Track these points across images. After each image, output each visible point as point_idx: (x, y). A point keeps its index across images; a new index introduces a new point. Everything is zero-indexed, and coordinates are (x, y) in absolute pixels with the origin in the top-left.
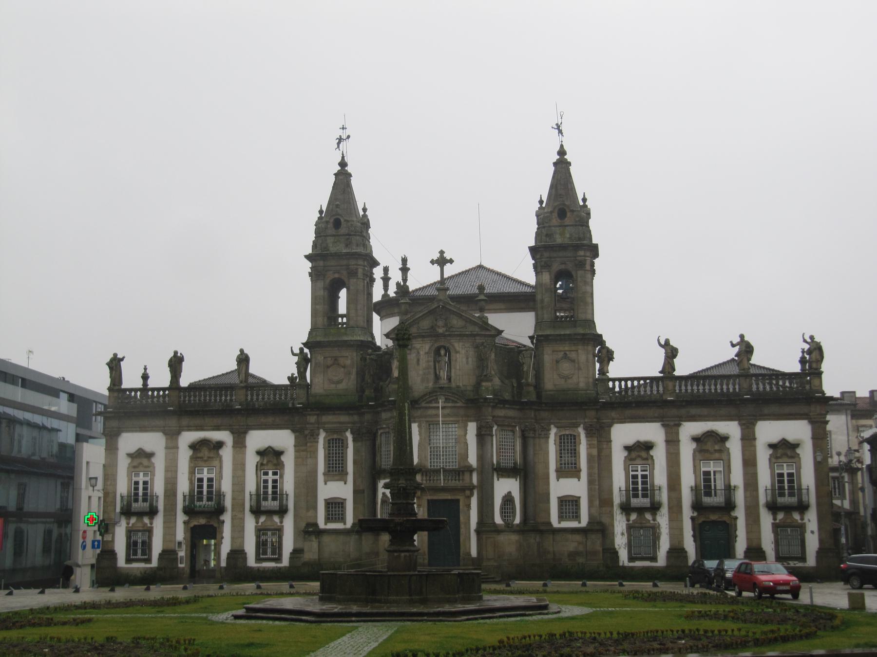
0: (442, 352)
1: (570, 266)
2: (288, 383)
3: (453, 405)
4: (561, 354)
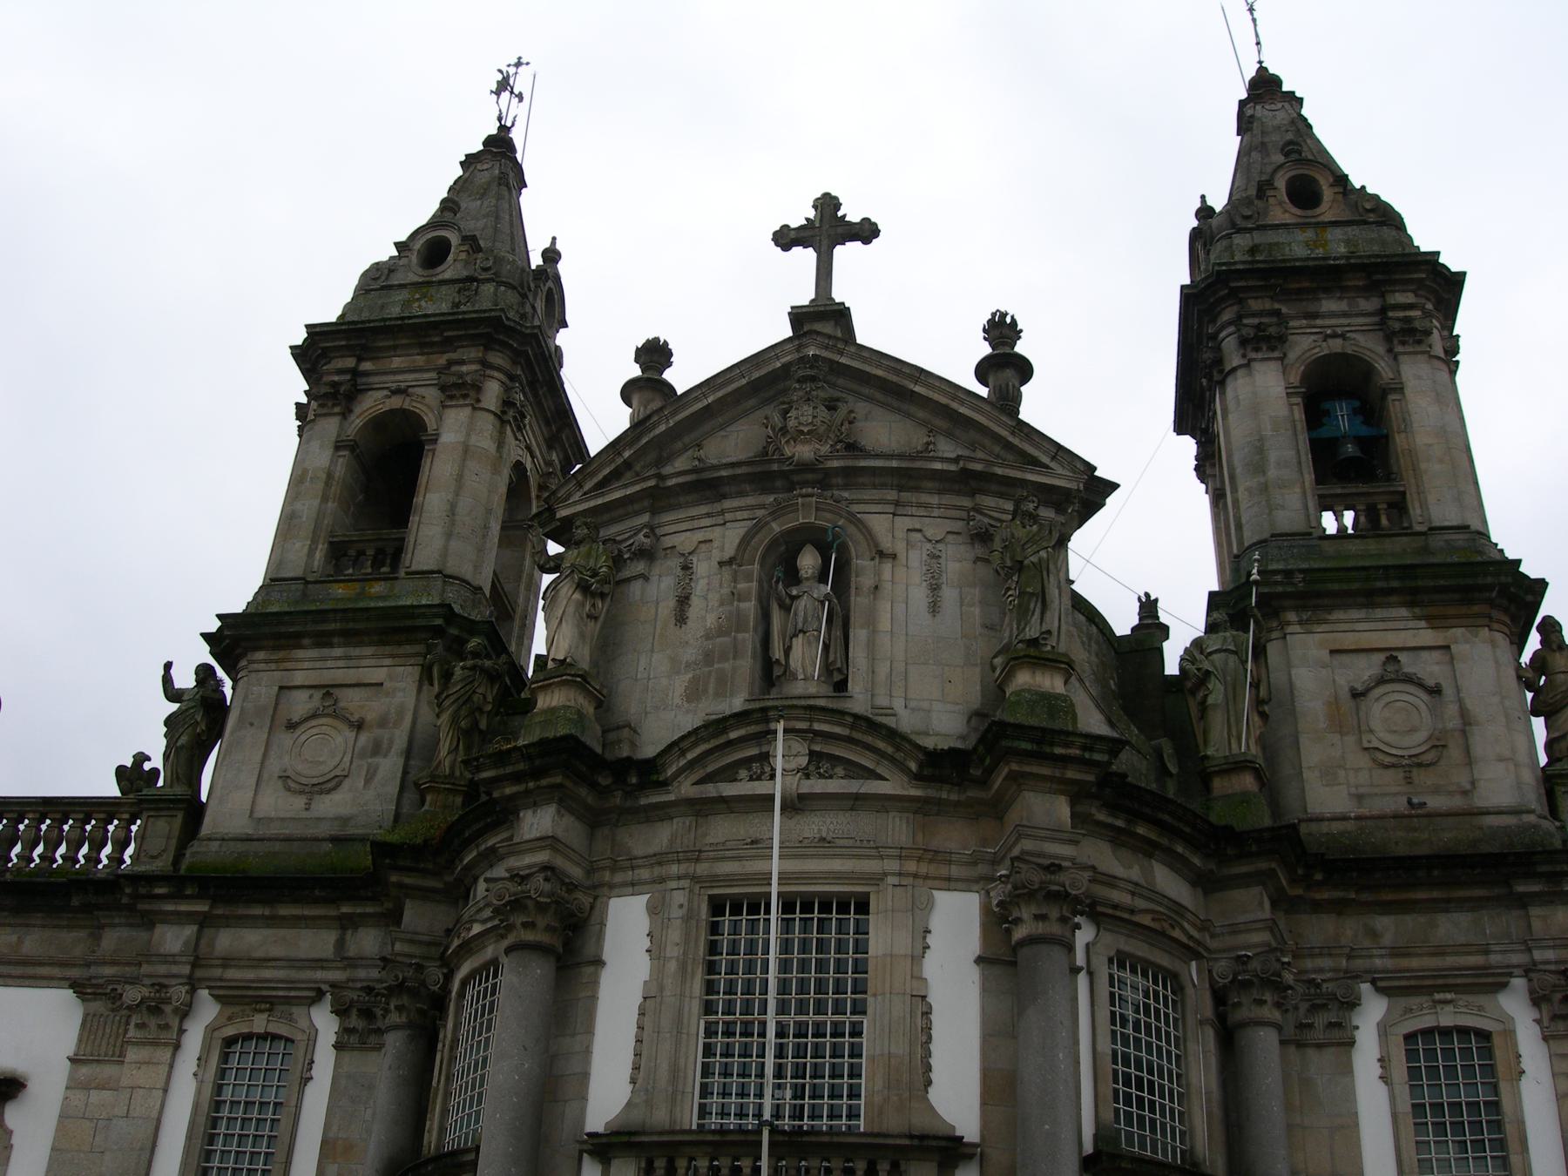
0: (808, 561)
1: (1369, 346)
2: (113, 791)
3: (854, 786)
4: (1365, 669)
